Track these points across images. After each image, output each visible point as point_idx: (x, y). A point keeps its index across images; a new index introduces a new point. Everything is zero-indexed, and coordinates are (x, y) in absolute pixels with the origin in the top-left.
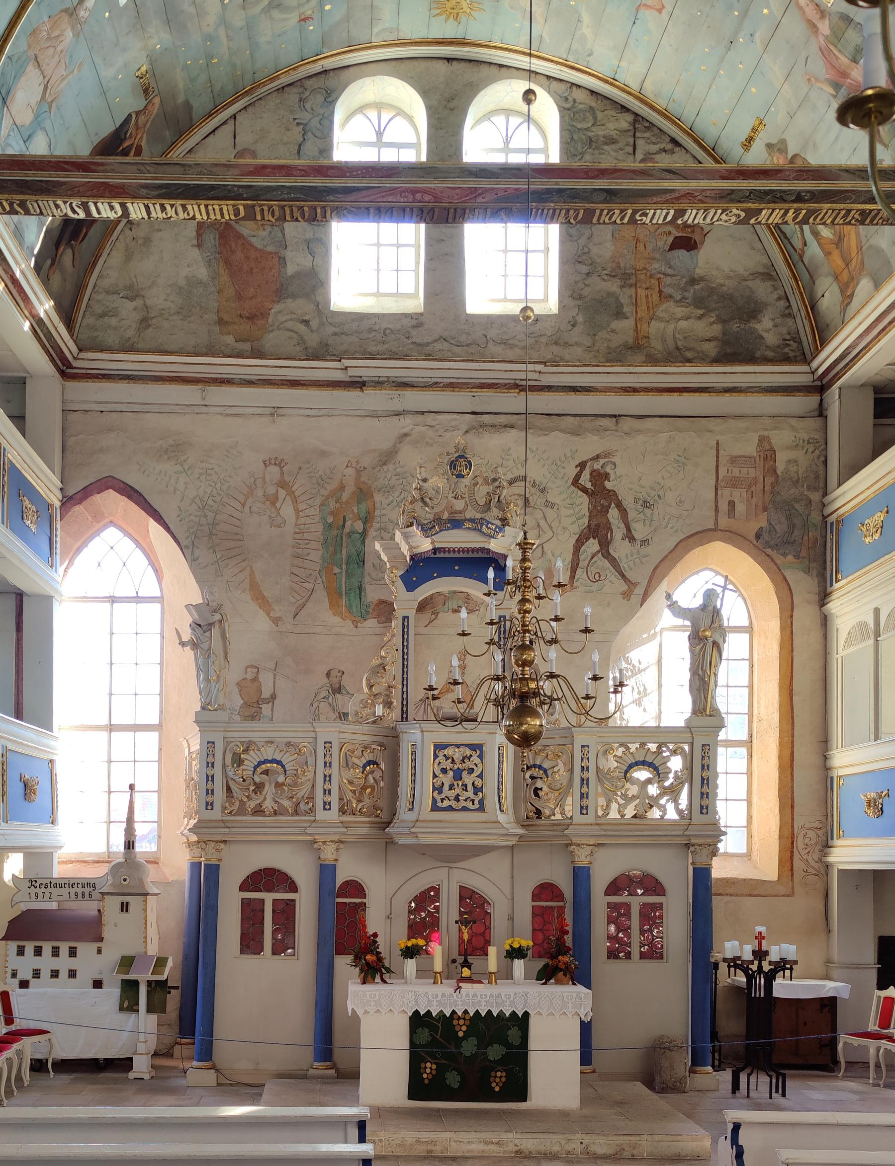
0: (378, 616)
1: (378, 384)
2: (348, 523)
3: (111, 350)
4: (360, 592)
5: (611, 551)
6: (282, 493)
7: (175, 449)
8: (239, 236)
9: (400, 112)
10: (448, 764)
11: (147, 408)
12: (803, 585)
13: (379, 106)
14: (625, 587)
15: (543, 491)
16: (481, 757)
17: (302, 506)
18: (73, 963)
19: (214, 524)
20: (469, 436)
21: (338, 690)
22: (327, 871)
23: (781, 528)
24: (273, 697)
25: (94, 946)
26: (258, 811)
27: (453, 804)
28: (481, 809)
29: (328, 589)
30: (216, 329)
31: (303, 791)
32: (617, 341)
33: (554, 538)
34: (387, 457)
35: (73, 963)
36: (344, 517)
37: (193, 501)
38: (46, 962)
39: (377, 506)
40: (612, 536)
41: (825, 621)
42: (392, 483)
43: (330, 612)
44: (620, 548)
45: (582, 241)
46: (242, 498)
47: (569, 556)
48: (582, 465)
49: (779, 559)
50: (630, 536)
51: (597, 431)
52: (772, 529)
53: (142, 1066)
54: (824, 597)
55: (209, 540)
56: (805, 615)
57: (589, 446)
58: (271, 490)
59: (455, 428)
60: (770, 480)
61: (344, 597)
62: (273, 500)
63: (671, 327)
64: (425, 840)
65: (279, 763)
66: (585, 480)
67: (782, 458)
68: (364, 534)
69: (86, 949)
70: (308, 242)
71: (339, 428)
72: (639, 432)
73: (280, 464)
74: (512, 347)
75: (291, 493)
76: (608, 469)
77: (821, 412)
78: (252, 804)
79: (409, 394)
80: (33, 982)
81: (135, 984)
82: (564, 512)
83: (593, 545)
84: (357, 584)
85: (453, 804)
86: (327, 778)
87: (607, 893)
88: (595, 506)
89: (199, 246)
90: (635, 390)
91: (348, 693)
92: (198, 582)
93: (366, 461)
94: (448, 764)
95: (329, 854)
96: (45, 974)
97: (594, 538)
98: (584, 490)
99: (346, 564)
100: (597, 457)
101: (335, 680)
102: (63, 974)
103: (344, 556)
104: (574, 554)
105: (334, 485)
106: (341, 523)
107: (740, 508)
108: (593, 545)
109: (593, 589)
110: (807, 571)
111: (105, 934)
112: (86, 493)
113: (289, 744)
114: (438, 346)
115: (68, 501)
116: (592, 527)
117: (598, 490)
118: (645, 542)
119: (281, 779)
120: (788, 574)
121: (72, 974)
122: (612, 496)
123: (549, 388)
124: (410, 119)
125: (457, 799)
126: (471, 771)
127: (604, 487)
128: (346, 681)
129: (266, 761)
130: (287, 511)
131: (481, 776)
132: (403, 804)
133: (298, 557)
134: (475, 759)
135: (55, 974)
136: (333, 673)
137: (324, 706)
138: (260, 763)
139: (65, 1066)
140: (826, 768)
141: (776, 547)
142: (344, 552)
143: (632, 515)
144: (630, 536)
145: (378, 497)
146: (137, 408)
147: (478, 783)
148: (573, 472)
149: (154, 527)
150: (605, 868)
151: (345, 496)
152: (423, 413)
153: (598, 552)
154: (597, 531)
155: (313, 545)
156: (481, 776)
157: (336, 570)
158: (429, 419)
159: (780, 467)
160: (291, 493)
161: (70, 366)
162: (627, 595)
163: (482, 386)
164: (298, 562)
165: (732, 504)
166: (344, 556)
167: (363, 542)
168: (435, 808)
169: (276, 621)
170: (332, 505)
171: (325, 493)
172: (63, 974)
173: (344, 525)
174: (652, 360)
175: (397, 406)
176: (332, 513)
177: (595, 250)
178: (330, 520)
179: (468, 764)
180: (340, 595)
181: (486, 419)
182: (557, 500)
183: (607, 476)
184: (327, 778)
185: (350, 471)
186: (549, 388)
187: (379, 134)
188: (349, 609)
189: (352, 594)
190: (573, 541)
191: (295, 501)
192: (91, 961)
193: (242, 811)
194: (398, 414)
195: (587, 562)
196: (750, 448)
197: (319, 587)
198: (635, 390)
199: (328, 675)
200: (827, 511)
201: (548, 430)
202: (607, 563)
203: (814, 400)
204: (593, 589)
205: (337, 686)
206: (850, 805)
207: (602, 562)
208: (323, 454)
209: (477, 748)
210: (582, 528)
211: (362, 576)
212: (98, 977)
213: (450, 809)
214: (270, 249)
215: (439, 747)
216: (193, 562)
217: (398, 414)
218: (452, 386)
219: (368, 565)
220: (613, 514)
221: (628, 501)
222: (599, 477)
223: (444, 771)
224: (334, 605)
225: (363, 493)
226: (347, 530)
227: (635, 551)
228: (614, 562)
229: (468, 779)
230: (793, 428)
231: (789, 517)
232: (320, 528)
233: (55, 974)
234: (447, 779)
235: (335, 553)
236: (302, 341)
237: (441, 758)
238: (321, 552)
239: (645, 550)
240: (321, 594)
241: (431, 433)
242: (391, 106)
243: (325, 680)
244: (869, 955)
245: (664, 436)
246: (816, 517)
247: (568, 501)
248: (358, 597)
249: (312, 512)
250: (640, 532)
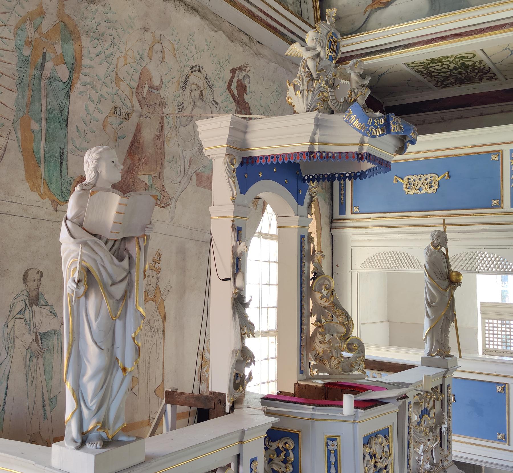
2: (49, 65)
4: (62, 163)
21: (35, 300)
36: (44, 55)
39: (85, 53)
42: (102, 28)
43: (27, 185)
61: (43, 166)
68: (69, 85)
84: (58, 151)
91: (47, 304)
99: (47, 120)
101: (32, 285)
103: (43, 109)
106: (40, 62)
136: (32, 275)
142: (44, 102)
145: (85, 42)
151: (46, 26)
157: (34, 126)
166: (43, 109)
167: (68, 95)
170: (31, 33)
171: (23, 13)
173: (43, 65)
176: (29, 43)
178: (27, 52)
180: (39, 163)
188: (48, 183)
189: (52, 164)
197: (14, 145)
199: (25, 277)
205: (35, 293)
211: (66, 143)
219: (72, 128)
224: (31, 175)
226: (47, 73)
232: (15, 60)
235: (31, 101)
238: (15, 95)
243: (22, 286)
248: (58, 169)
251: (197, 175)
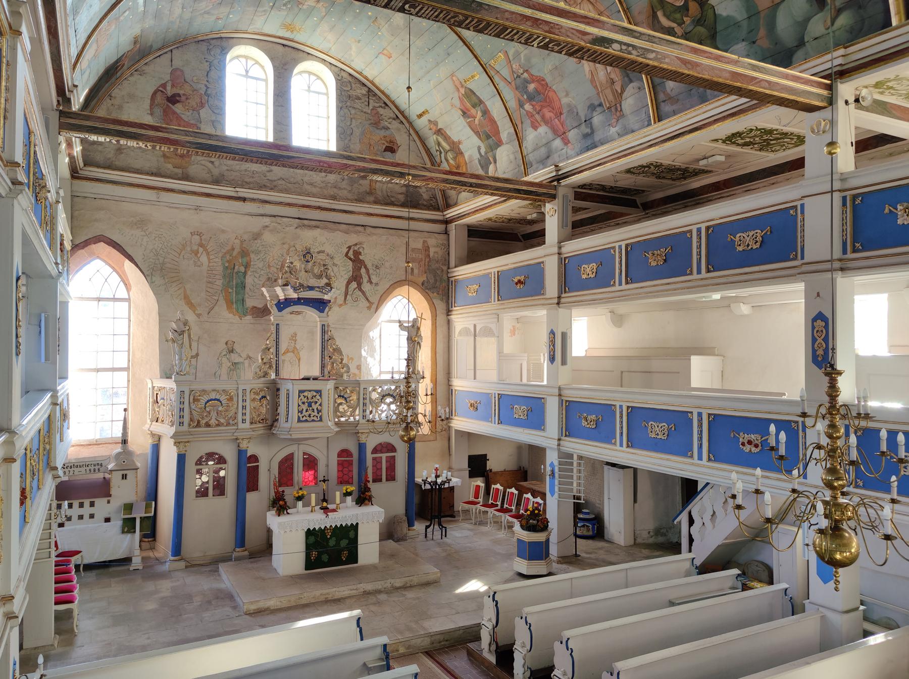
0: (252, 314)
1: (253, 200)
2: (236, 267)
3: (98, 166)
6: (201, 250)
7: (141, 223)
8: (174, 113)
9: (257, 63)
10: (305, 400)
11: (123, 199)
12: (441, 306)
13: (247, 58)
14: (368, 305)
16: (320, 396)
17: (211, 257)
18: (92, 510)
19: (163, 264)
20: (298, 230)
21: (231, 351)
22: (241, 453)
23: (432, 281)
24: (197, 355)
25: (106, 499)
26: (208, 425)
27: (308, 418)
28: (321, 420)
29: (225, 299)
30: (162, 160)
31: (231, 414)
32: (362, 189)
34: (257, 236)
35: (92, 510)
37: (151, 251)
38: (76, 511)
41: (449, 322)
42: (260, 249)
44: (366, 287)
45: (346, 141)
46: (179, 251)
47: (344, 289)
48: (349, 248)
49: (431, 295)
50: (370, 281)
51: (356, 232)
52: (428, 281)
53: (137, 562)
54: (448, 312)
55: (161, 273)
56: (441, 318)
57: (353, 239)
58: (195, 248)
59: (291, 225)
60: (427, 260)
62: (196, 253)
63: (385, 186)
64: (294, 436)
65: (218, 400)
66: (351, 254)
67: (432, 250)
68: (245, 273)
69: (100, 502)
70: (213, 122)
71: (229, 220)
72: (374, 234)
73: (200, 234)
74: (315, 186)
75: (206, 250)
76: (361, 250)
77: (446, 232)
78: (203, 422)
79: (268, 206)
80: (67, 523)
81: (135, 519)
82: (341, 269)
83: (354, 285)
85: (308, 418)
86: (244, 407)
87: (372, 453)
89: (152, 114)
90: (371, 215)
92: (155, 294)
93: (246, 237)
94: (305, 400)
95: (244, 445)
96: (75, 518)
98: (350, 259)
100: (356, 244)
102: (86, 517)
105: (229, 248)
107: (416, 271)
108: (354, 285)
110: (442, 300)
111: (112, 492)
112: (86, 243)
113: (223, 390)
114: (280, 182)
115: (76, 247)
117: (356, 259)
118: (377, 284)
119: (220, 408)
120: (435, 301)
121: (92, 516)
122: (362, 262)
123: (334, 210)
124: (262, 67)
125: (310, 416)
126: (316, 403)
128: (236, 347)
129: (211, 400)
130: (204, 259)
131: (320, 405)
132: (282, 418)
133: (210, 282)
134: (318, 397)
135: (81, 517)
137: (224, 360)
138: (208, 401)
139: (89, 567)
140: (449, 385)
141: (429, 289)
143: (371, 272)
144: (370, 281)
145: (252, 256)
146: (117, 198)
147: (319, 408)
149: (128, 264)
150: (372, 442)
151: (235, 253)
152: (274, 216)
154: (356, 278)
155: (217, 277)
156: (320, 405)
157: (230, 290)
158: (278, 219)
159: (431, 254)
160: (206, 250)
161: (77, 173)
162: (369, 308)
163: (304, 206)
164: (209, 285)
165: (412, 269)
167: (245, 277)
168: (299, 421)
169: (199, 316)
170: (228, 257)
172: (86, 517)
174: (376, 202)
175: (261, 211)
177: (352, 146)
178: (227, 265)
179: (315, 399)
181: (305, 222)
182: (338, 263)
183: (360, 253)
184: (244, 407)
185: (237, 241)
186: (334, 210)
187: (247, 71)
188: (237, 310)
190: (345, 282)
191: (208, 254)
192: (102, 507)
193: (198, 425)
194: (262, 215)
196: (419, 245)
198: (371, 215)
199: (226, 343)
200: (450, 275)
201: (334, 230)
203: (444, 226)
206: (461, 404)
207: (358, 293)
208: (223, 231)
209: (319, 392)
212: (108, 516)
213: (306, 421)
214: (192, 122)
215: (301, 392)
216: (151, 283)
217: (262, 215)
218: (289, 205)
219: (247, 289)
220: (363, 271)
221: (369, 266)
222: (357, 253)
223: (303, 403)
225: (244, 253)
226: (236, 270)
228: (363, 293)
229: (314, 407)
230: (436, 238)
231: (435, 277)
233: (81, 517)
234: (305, 407)
236: (210, 171)
237: (302, 397)
239: (376, 288)
240: (222, 302)
241: (279, 227)
242: (253, 59)
244: (465, 464)
245: (384, 237)
246: (445, 277)
249: (217, 260)
250: (374, 279)
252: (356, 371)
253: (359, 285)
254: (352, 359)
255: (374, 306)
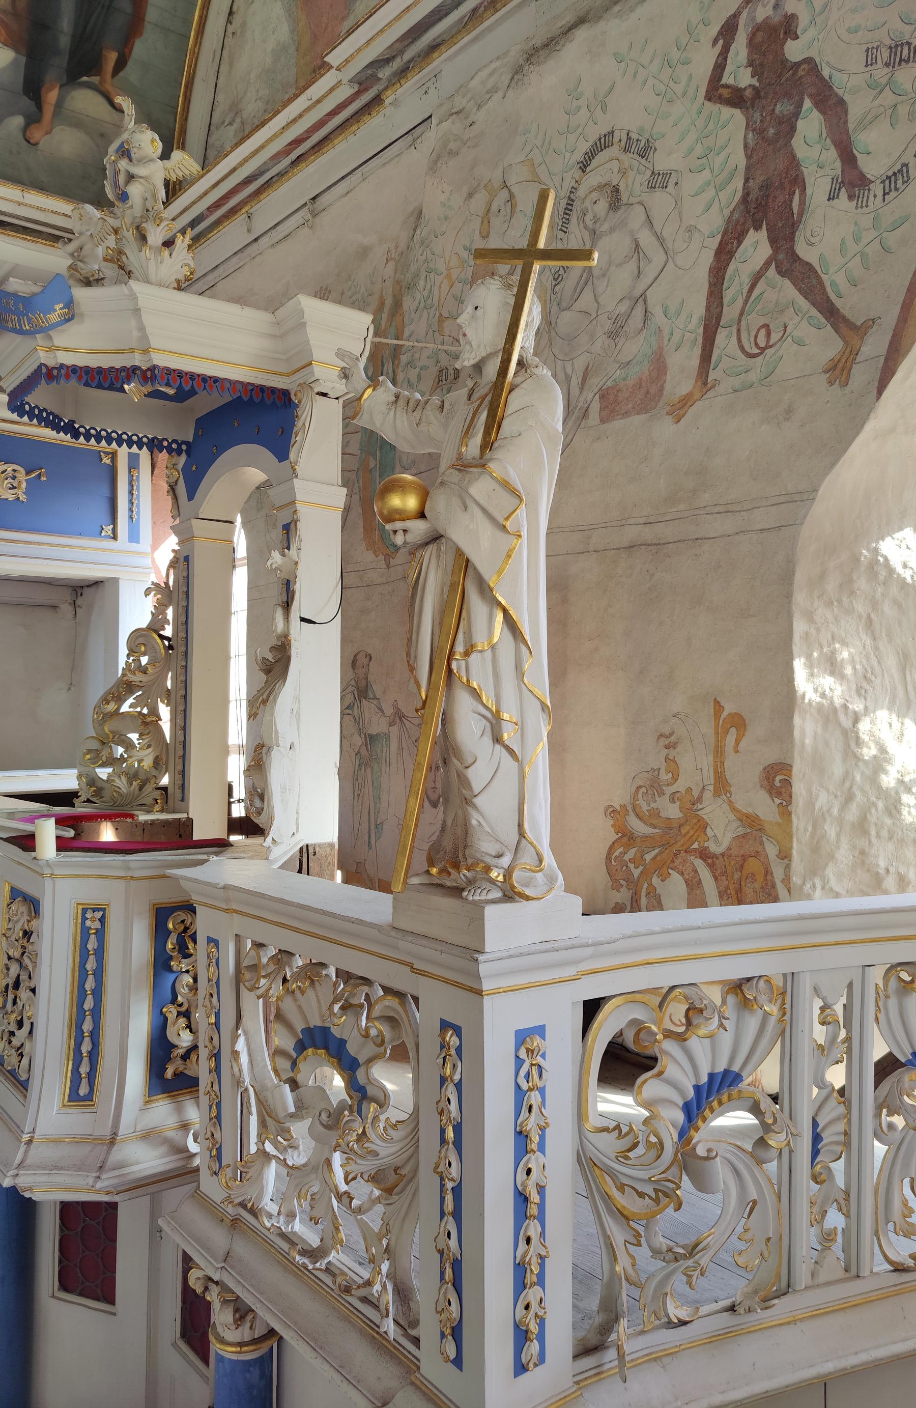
5: (801, 249)
14: (833, 346)
15: (644, 153)
33: (670, 265)
39: (406, 321)
40: (802, 202)
83: (756, 247)
88: (760, 132)
91: (375, 698)
97: (757, 228)
104: (711, 294)
108: (756, 247)
109: (753, 377)
116: (754, 195)
118: (898, 177)
127: (784, 61)
136: (362, 660)
144: (853, 182)
148: (704, 59)
153: (767, 264)
195: (740, 303)
202: (788, 290)
204: (753, 377)
205: (363, 683)
210: (727, 212)
227: (866, 221)
247: (699, 150)
251: (602, 397)
252: (764, 807)
253: (783, 237)
254: (739, 723)
255: (874, 346)
